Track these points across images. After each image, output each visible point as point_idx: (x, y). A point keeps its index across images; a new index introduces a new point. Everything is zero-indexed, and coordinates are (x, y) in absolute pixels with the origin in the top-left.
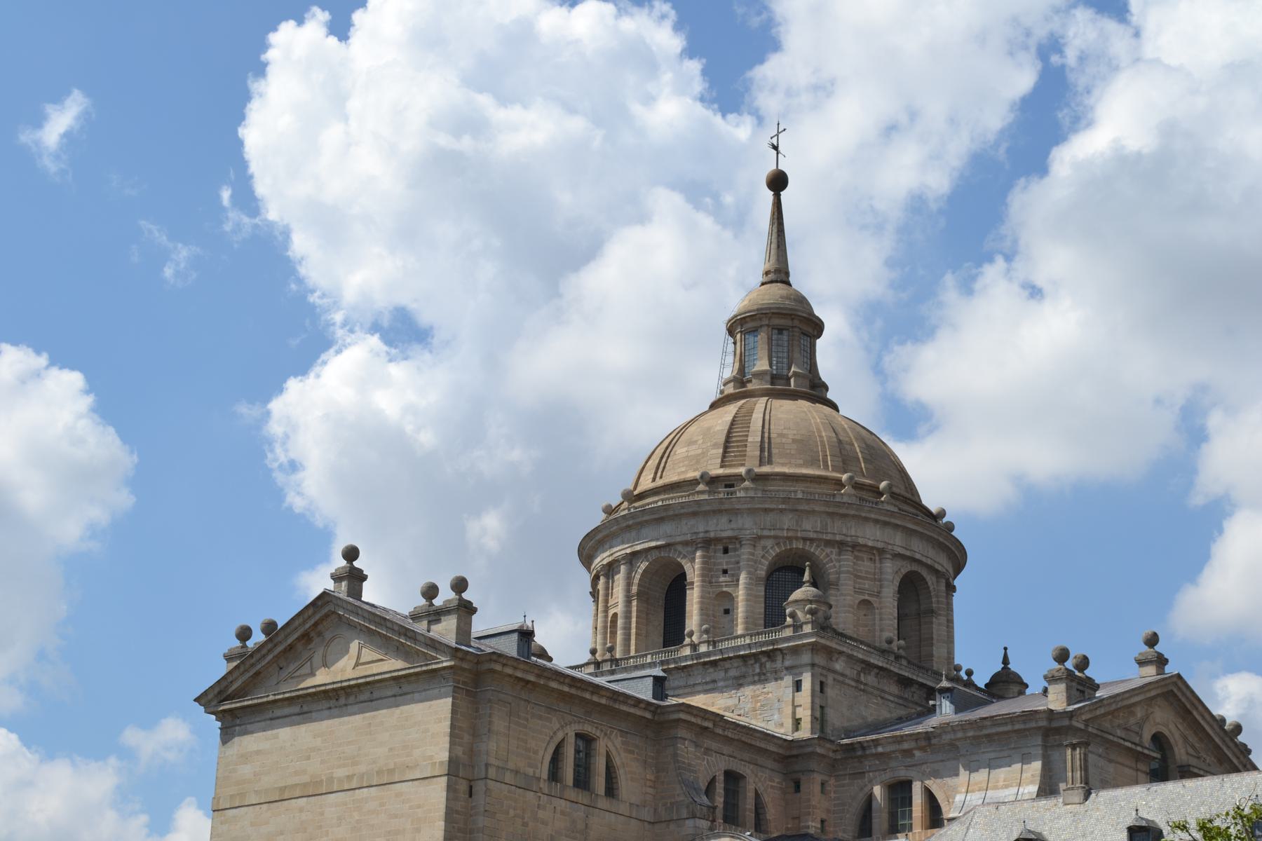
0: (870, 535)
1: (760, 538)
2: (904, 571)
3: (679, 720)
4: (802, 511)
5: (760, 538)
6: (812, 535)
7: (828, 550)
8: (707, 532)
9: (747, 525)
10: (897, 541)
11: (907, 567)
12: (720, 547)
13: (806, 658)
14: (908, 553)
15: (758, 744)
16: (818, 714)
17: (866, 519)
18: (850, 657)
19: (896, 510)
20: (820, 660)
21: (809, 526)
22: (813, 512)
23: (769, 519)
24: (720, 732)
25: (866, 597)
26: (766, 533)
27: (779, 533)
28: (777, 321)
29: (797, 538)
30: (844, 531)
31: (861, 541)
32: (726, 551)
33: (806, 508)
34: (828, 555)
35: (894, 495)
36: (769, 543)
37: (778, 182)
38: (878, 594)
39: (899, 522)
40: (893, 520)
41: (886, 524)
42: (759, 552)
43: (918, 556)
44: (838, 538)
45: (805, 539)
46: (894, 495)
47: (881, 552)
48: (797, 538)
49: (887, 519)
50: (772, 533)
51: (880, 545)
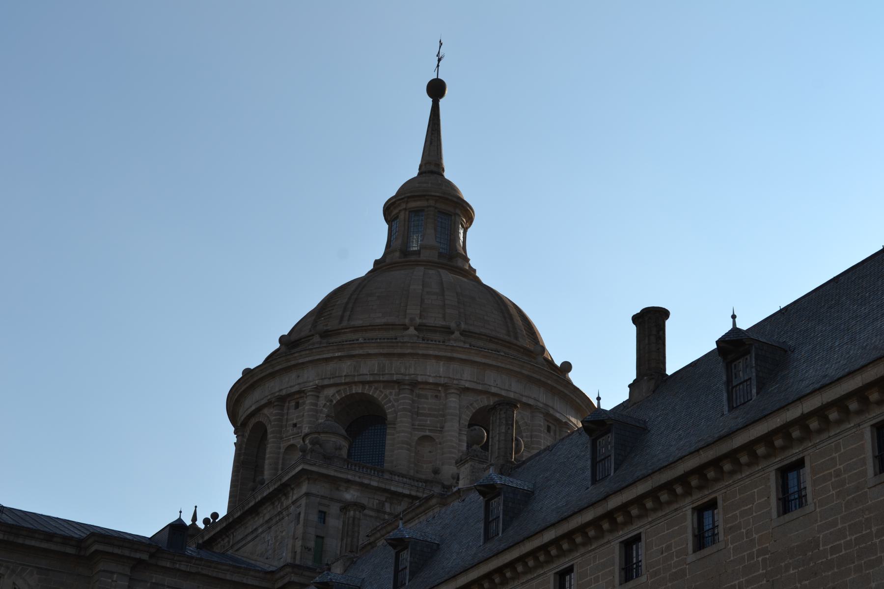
0: (432, 371)
1: (324, 387)
2: (477, 406)
3: (96, 551)
4: (360, 356)
5: (324, 387)
6: (369, 378)
7: (387, 392)
8: (281, 390)
9: (310, 377)
10: (467, 376)
11: (485, 402)
12: (293, 403)
13: (304, 489)
14: (480, 387)
15: (228, 577)
16: (312, 544)
17: (426, 356)
18: (362, 485)
19: (467, 346)
20: (320, 489)
21: (368, 368)
22: (368, 356)
23: (330, 367)
24: (168, 565)
25: (428, 433)
26: (326, 382)
27: (337, 381)
28: (413, 205)
29: (355, 383)
30: (403, 371)
31: (420, 379)
32: (297, 406)
33: (361, 352)
34: (386, 396)
35: (463, 333)
36: (330, 392)
37: (436, 89)
38: (441, 430)
39: (463, 357)
40: (455, 355)
41: (451, 359)
42: (322, 402)
43: (493, 390)
44: (395, 378)
45: (363, 383)
46: (463, 333)
47: (446, 386)
48: (355, 383)
49: (449, 354)
50: (332, 381)
51: (442, 381)
